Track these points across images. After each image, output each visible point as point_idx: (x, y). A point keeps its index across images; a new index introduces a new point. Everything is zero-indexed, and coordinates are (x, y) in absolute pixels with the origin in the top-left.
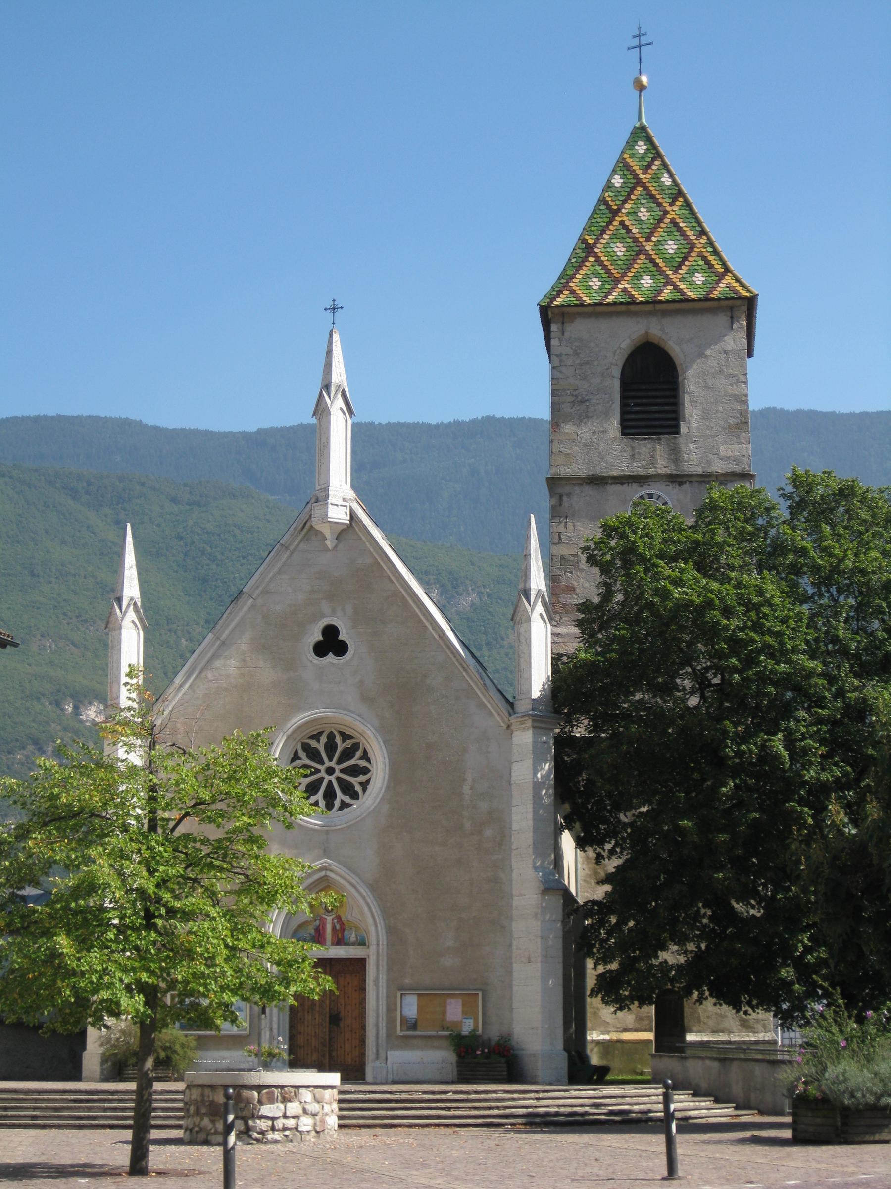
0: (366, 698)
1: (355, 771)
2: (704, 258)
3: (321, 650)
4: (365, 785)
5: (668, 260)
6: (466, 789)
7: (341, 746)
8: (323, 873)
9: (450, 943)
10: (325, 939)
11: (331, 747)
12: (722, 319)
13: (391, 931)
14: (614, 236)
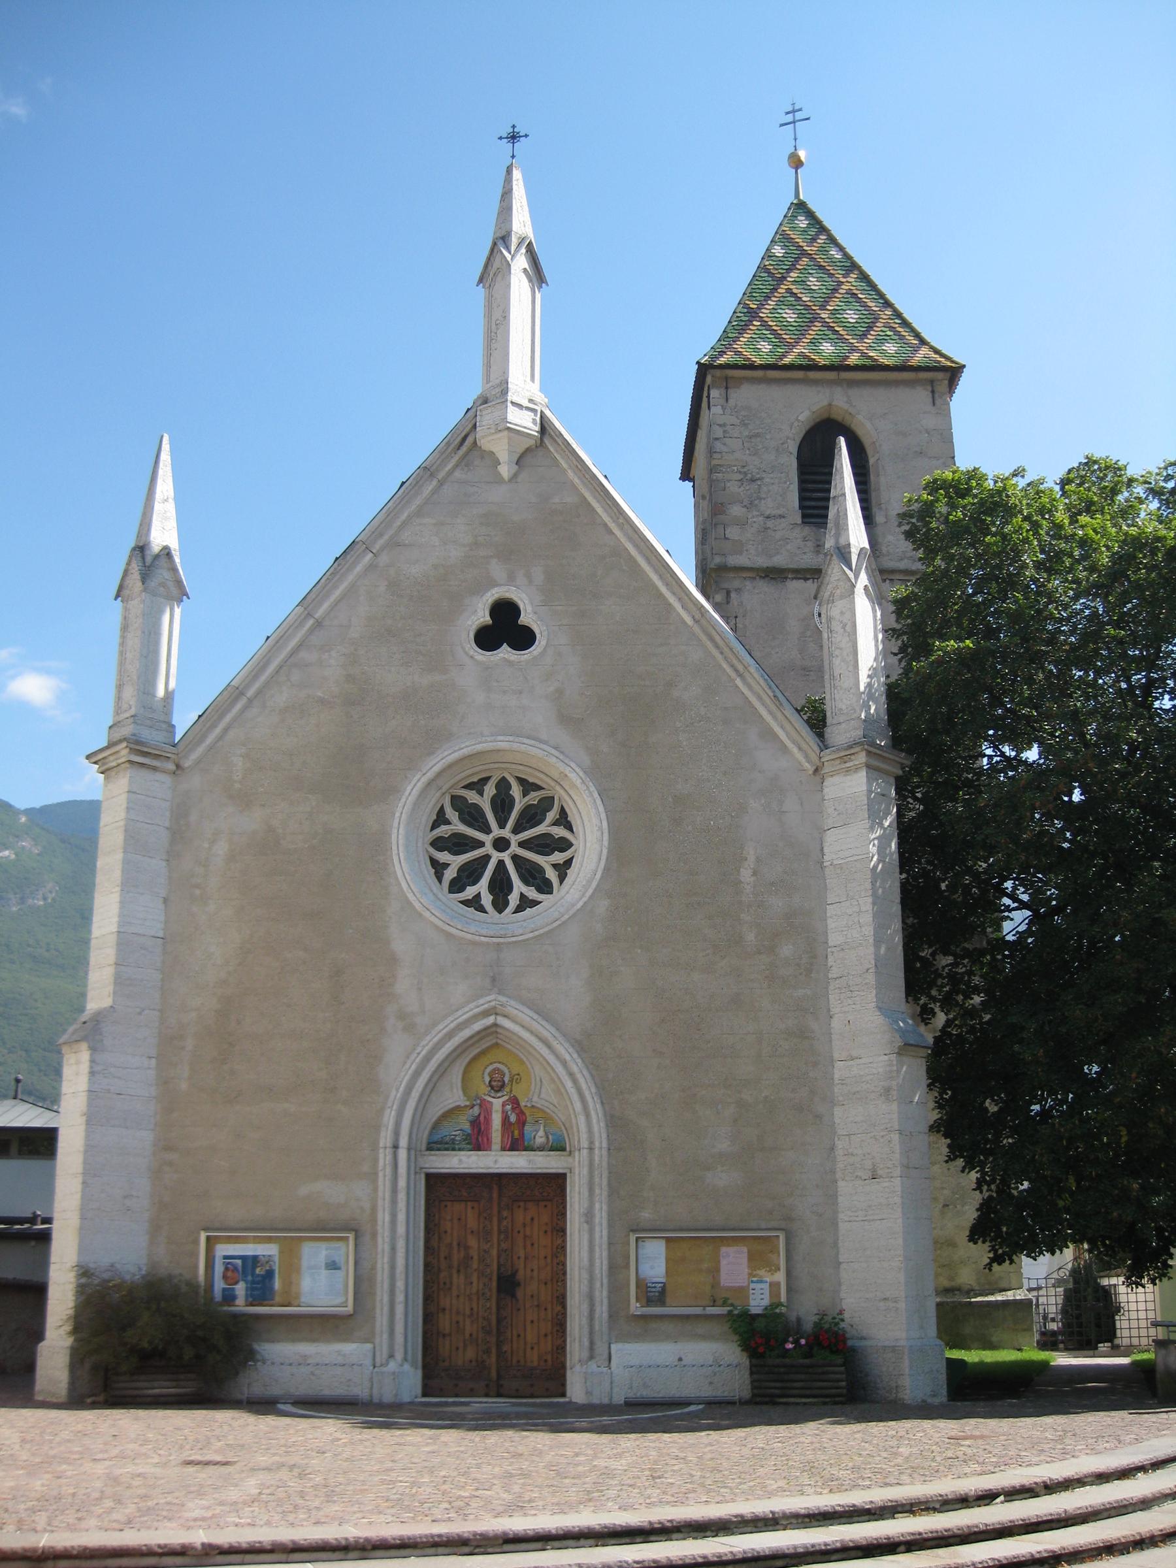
0: (565, 719)
1: (546, 845)
2: (892, 329)
3: (487, 639)
4: (563, 869)
5: (851, 329)
6: (746, 875)
7: (520, 802)
8: (491, 1020)
9: (724, 1146)
10: (489, 1141)
11: (502, 804)
12: (921, 395)
13: (614, 1122)
14: (781, 303)
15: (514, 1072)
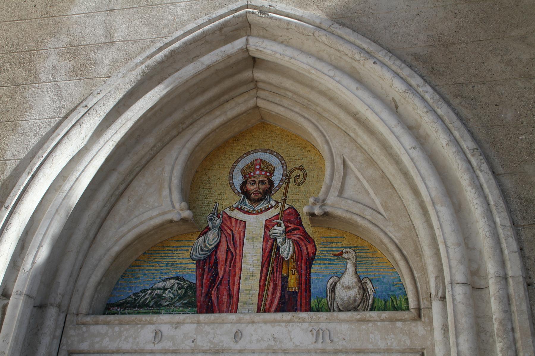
15: (291, 166)
